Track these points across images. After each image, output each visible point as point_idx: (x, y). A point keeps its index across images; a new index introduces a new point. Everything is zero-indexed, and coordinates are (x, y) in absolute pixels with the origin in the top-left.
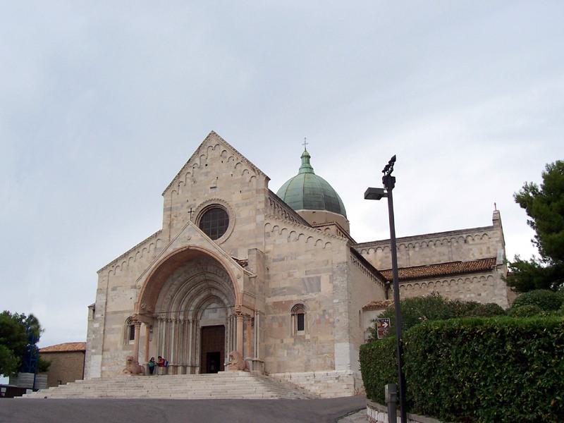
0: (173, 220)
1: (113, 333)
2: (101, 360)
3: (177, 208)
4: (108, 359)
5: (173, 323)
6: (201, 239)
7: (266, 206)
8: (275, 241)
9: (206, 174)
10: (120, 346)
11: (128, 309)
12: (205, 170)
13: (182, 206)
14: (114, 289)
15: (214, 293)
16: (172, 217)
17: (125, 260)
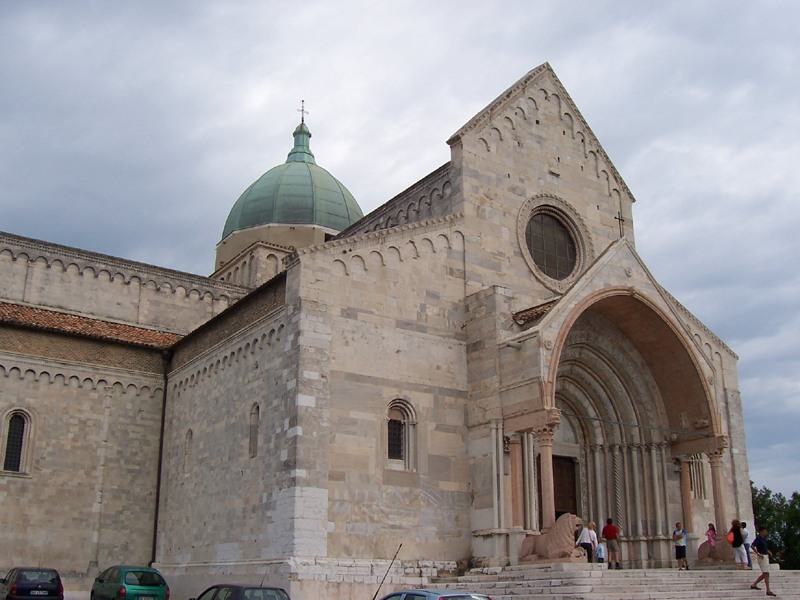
0: (483, 202)
1: (354, 434)
2: (326, 504)
4: (342, 502)
9: (540, 140)
10: (374, 471)
11: (392, 377)
12: (534, 129)
13: (499, 180)
14: (349, 313)
16: (481, 191)
17: (378, 248)
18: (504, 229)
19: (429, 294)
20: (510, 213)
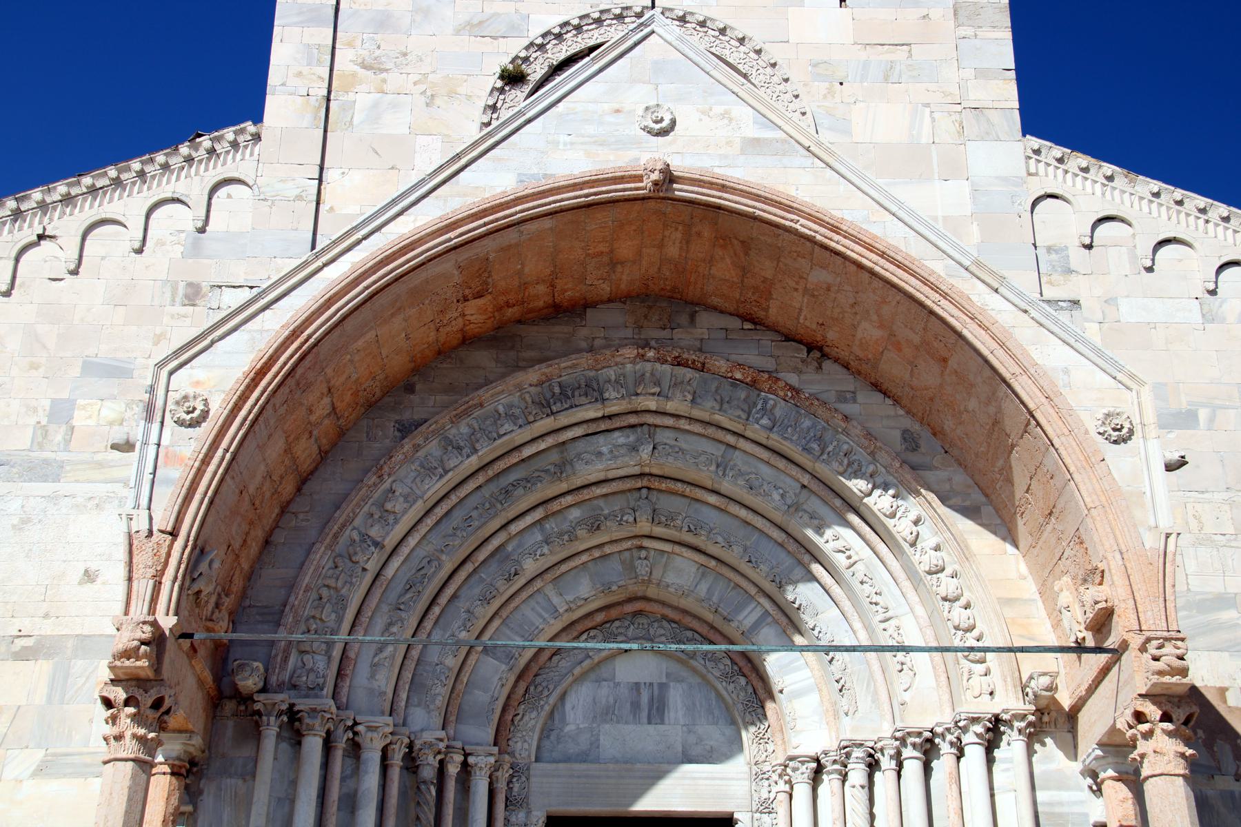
5: (372, 758)
6: (753, 145)
8: (1110, 301)
15: (680, 576)
18: (422, 140)
19: (91, 368)
20: (452, 94)
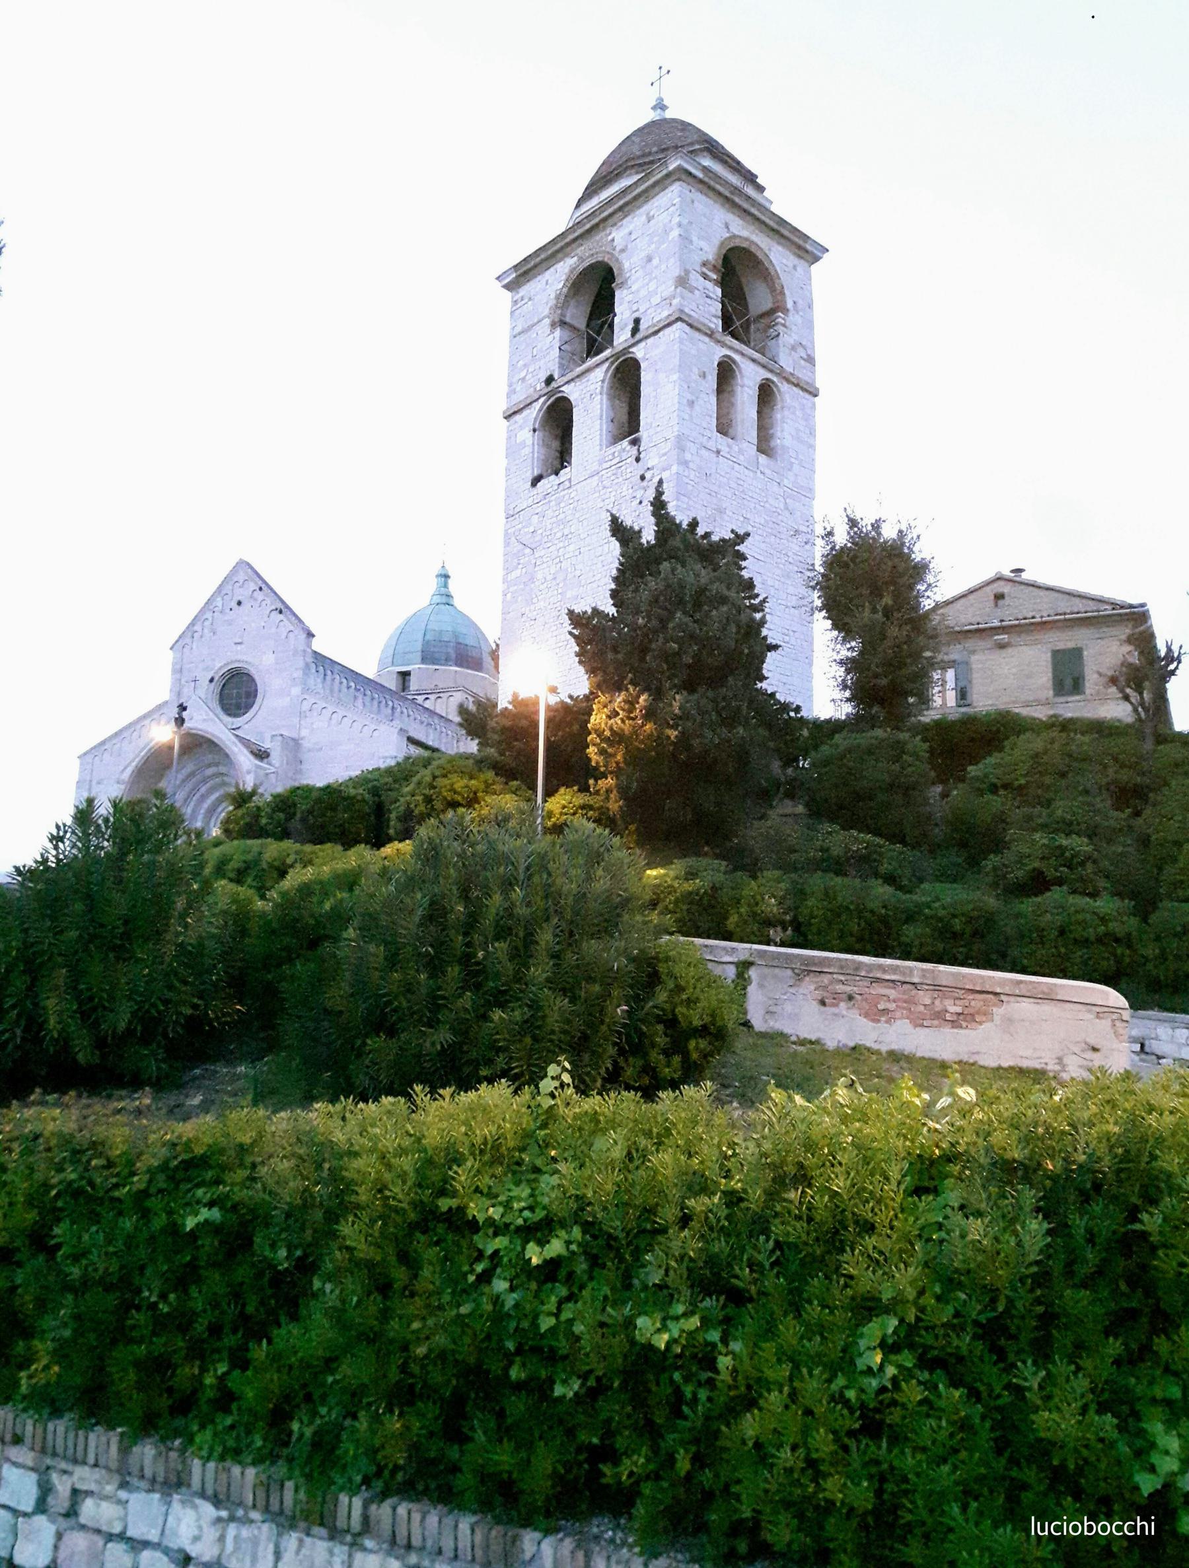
3: (190, 671)
7: (305, 674)
9: (230, 623)
12: (230, 616)
